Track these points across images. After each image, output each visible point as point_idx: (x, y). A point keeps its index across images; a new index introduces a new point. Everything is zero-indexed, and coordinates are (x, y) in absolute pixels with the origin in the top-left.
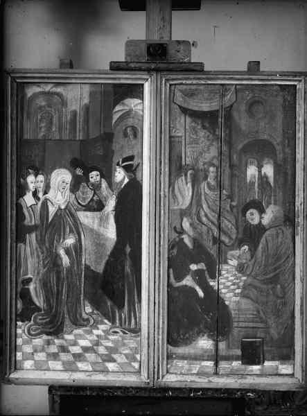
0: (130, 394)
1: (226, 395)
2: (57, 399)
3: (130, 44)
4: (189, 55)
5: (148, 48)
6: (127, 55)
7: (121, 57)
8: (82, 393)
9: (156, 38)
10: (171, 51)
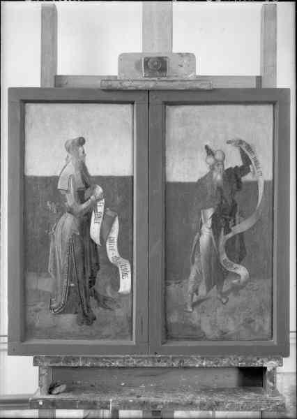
0: (130, 364)
1: (244, 363)
2: (44, 372)
3: (123, 58)
4: (194, 69)
5: (146, 63)
6: (121, 70)
8: (73, 365)
9: (156, 51)
10: (172, 65)
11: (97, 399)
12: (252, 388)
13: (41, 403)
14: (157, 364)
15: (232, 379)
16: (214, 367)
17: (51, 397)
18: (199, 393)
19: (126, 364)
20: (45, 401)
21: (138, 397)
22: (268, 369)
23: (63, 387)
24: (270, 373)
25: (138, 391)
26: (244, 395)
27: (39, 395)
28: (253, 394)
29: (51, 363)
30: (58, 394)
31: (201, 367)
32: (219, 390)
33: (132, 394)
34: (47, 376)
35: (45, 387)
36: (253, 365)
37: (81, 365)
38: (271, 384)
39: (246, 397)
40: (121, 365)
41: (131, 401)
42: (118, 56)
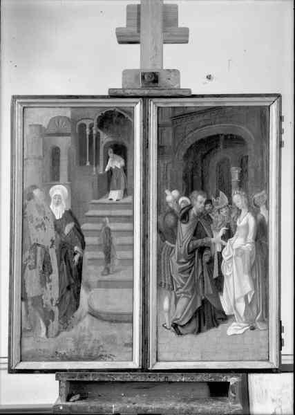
0: (128, 380)
2: (64, 385)
3: (125, 73)
5: (143, 77)
6: (124, 82)
7: (118, 84)
8: (85, 379)
9: (150, 68)
10: (163, 79)
11: (103, 405)
12: (220, 398)
13: (61, 408)
14: (148, 379)
15: (205, 391)
16: (191, 382)
17: (69, 404)
18: (179, 401)
19: (125, 379)
20: (64, 406)
21: (134, 404)
22: (231, 384)
23: (78, 396)
24: (232, 386)
25: (133, 399)
26: (213, 403)
27: (59, 402)
28: (220, 403)
29: (69, 378)
30: (74, 401)
31: (181, 382)
32: (193, 400)
33: (129, 402)
34: (66, 388)
35: (64, 396)
36: (220, 380)
37: (91, 380)
38: (233, 395)
39: (214, 404)
40: (121, 380)
41: (128, 407)
42: (122, 70)
